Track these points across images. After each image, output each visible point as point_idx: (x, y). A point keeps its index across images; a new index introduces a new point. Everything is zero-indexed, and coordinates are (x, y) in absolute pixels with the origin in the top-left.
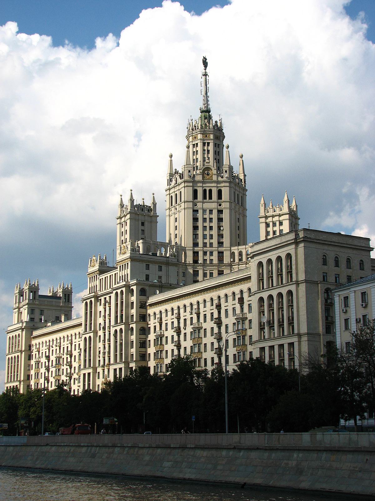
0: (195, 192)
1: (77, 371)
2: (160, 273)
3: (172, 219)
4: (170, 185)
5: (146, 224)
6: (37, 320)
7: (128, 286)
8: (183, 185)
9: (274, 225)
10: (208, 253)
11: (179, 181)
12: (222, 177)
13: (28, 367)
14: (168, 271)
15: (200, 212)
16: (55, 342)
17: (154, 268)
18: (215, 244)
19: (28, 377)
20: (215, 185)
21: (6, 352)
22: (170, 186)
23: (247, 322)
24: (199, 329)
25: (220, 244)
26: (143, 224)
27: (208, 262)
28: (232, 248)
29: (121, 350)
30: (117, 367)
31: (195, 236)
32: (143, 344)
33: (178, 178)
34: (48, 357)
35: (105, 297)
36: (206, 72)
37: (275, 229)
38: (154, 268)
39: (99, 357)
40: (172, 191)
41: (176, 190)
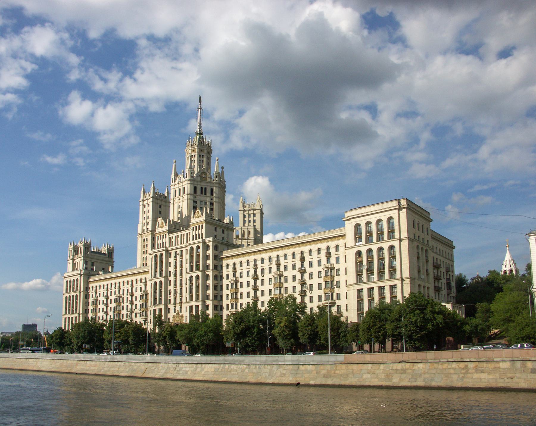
0: (195, 188)
1: (138, 307)
2: (224, 235)
3: (176, 206)
4: (175, 182)
5: (162, 207)
6: (89, 269)
7: (204, 242)
8: (187, 182)
9: (250, 215)
11: (183, 179)
13: (87, 304)
14: (228, 235)
15: (198, 202)
16: (113, 286)
17: (219, 230)
19: (86, 311)
20: (208, 184)
21: (63, 292)
22: (175, 183)
23: (334, 272)
24: (281, 276)
26: (160, 207)
29: (197, 291)
30: (194, 304)
32: (218, 287)
33: (182, 177)
34: (107, 297)
35: (176, 251)
37: (250, 219)
38: (219, 230)
39: (170, 297)
40: (175, 187)
41: (179, 186)
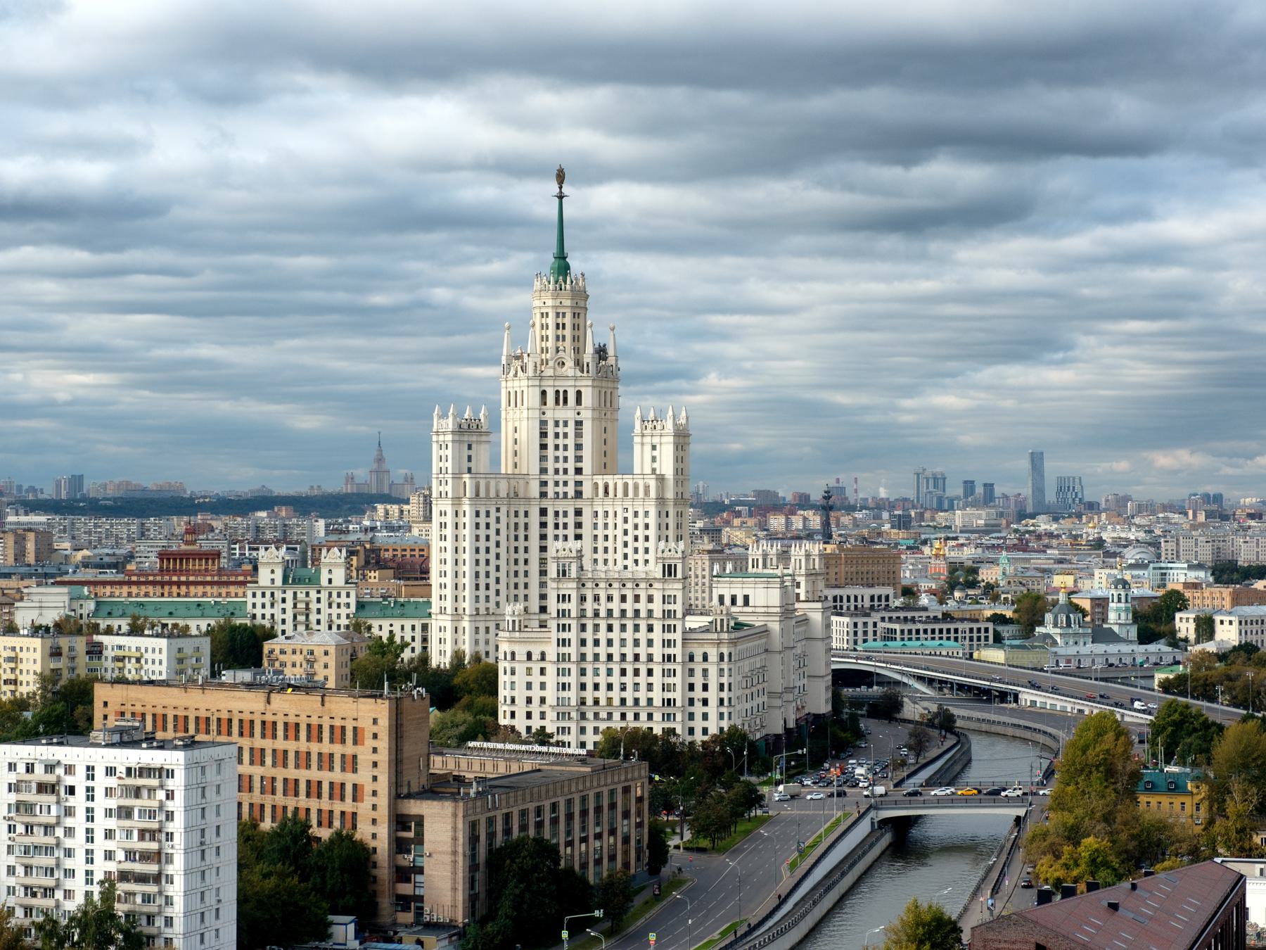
0: (544, 393)
5: (474, 446)
10: (561, 484)
12: (583, 372)
18: (571, 471)
20: (572, 383)
25: (579, 471)
26: (470, 447)
27: (561, 496)
28: (595, 477)
31: (543, 458)
33: (519, 368)
36: (561, 192)
